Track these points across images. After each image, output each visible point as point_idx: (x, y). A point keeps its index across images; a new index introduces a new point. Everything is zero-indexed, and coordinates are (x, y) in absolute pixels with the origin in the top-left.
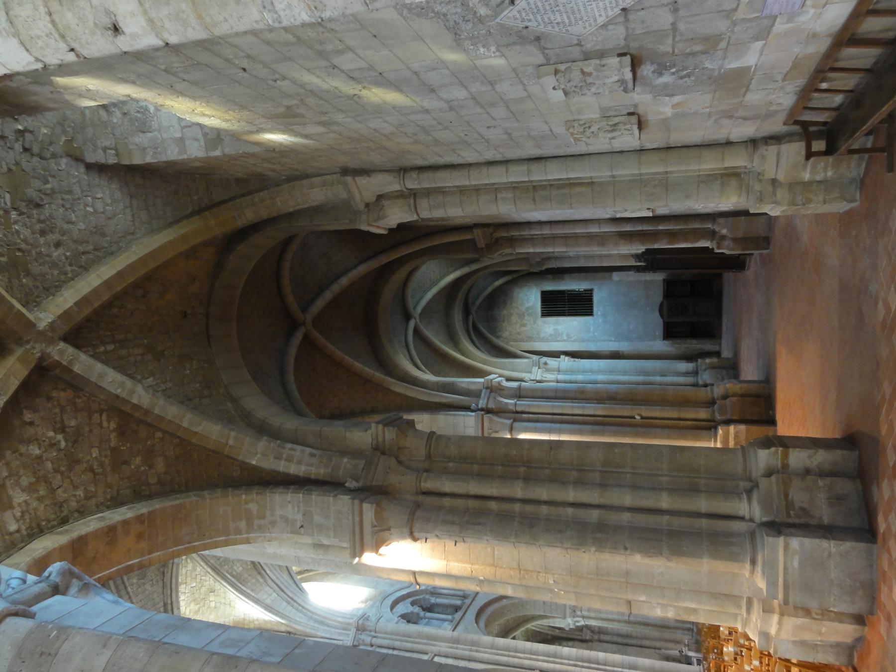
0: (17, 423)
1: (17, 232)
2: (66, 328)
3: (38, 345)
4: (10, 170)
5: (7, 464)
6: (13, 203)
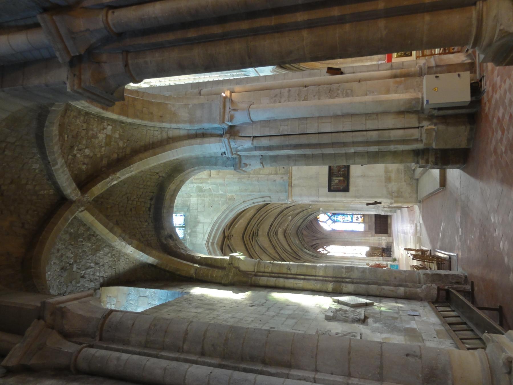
0: (90, 166)
1: (72, 253)
2: (73, 207)
3: (85, 200)
4: (71, 282)
5: (100, 152)
6: (73, 268)
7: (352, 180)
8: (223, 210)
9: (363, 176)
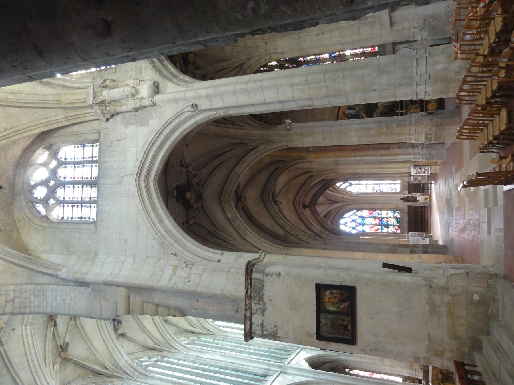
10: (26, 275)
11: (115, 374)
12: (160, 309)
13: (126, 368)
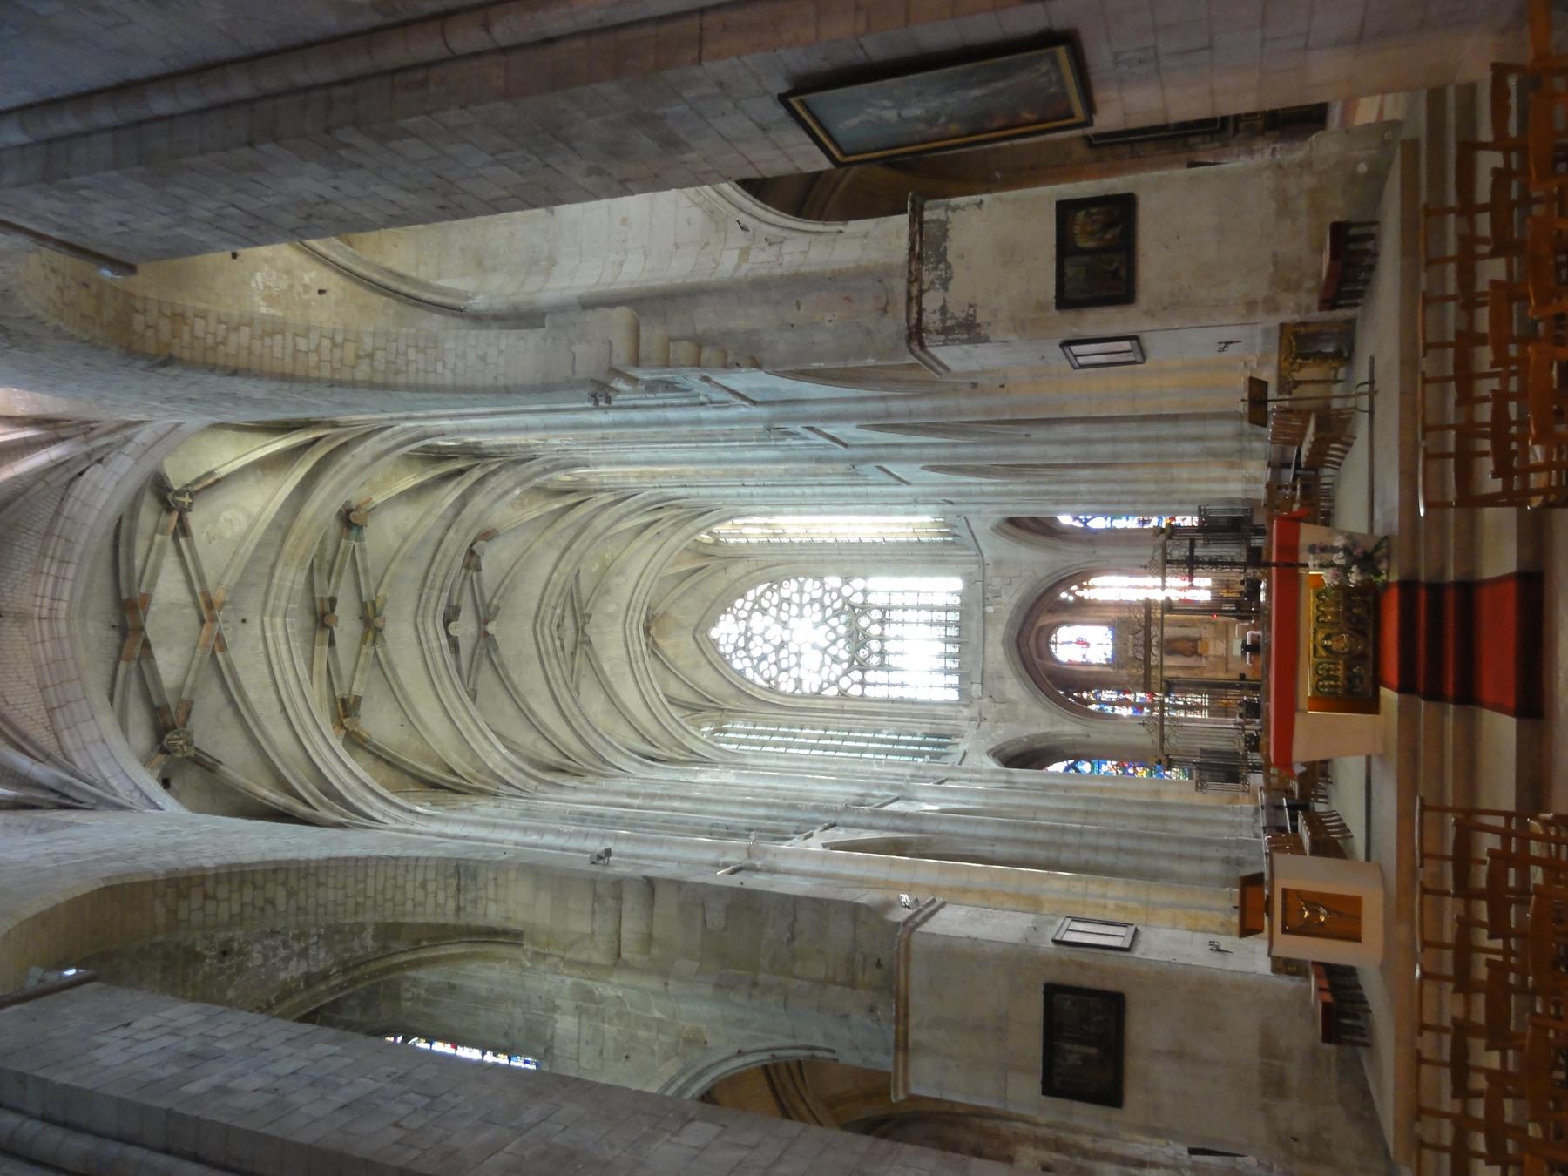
7: (1134, 1063)
8: (666, 1079)
9: (1178, 1055)
10: (391, 312)
11: (477, 785)
12: (706, 353)
13: (504, 770)
